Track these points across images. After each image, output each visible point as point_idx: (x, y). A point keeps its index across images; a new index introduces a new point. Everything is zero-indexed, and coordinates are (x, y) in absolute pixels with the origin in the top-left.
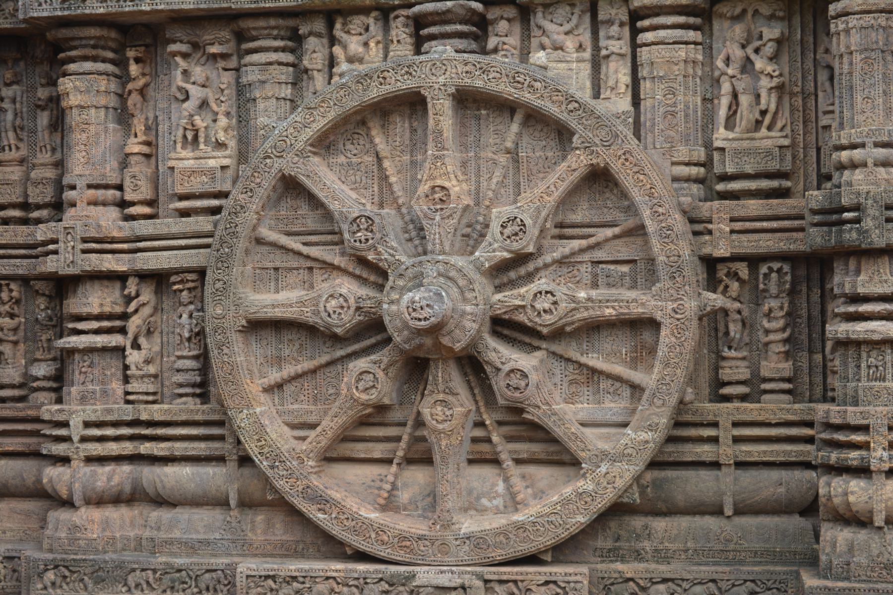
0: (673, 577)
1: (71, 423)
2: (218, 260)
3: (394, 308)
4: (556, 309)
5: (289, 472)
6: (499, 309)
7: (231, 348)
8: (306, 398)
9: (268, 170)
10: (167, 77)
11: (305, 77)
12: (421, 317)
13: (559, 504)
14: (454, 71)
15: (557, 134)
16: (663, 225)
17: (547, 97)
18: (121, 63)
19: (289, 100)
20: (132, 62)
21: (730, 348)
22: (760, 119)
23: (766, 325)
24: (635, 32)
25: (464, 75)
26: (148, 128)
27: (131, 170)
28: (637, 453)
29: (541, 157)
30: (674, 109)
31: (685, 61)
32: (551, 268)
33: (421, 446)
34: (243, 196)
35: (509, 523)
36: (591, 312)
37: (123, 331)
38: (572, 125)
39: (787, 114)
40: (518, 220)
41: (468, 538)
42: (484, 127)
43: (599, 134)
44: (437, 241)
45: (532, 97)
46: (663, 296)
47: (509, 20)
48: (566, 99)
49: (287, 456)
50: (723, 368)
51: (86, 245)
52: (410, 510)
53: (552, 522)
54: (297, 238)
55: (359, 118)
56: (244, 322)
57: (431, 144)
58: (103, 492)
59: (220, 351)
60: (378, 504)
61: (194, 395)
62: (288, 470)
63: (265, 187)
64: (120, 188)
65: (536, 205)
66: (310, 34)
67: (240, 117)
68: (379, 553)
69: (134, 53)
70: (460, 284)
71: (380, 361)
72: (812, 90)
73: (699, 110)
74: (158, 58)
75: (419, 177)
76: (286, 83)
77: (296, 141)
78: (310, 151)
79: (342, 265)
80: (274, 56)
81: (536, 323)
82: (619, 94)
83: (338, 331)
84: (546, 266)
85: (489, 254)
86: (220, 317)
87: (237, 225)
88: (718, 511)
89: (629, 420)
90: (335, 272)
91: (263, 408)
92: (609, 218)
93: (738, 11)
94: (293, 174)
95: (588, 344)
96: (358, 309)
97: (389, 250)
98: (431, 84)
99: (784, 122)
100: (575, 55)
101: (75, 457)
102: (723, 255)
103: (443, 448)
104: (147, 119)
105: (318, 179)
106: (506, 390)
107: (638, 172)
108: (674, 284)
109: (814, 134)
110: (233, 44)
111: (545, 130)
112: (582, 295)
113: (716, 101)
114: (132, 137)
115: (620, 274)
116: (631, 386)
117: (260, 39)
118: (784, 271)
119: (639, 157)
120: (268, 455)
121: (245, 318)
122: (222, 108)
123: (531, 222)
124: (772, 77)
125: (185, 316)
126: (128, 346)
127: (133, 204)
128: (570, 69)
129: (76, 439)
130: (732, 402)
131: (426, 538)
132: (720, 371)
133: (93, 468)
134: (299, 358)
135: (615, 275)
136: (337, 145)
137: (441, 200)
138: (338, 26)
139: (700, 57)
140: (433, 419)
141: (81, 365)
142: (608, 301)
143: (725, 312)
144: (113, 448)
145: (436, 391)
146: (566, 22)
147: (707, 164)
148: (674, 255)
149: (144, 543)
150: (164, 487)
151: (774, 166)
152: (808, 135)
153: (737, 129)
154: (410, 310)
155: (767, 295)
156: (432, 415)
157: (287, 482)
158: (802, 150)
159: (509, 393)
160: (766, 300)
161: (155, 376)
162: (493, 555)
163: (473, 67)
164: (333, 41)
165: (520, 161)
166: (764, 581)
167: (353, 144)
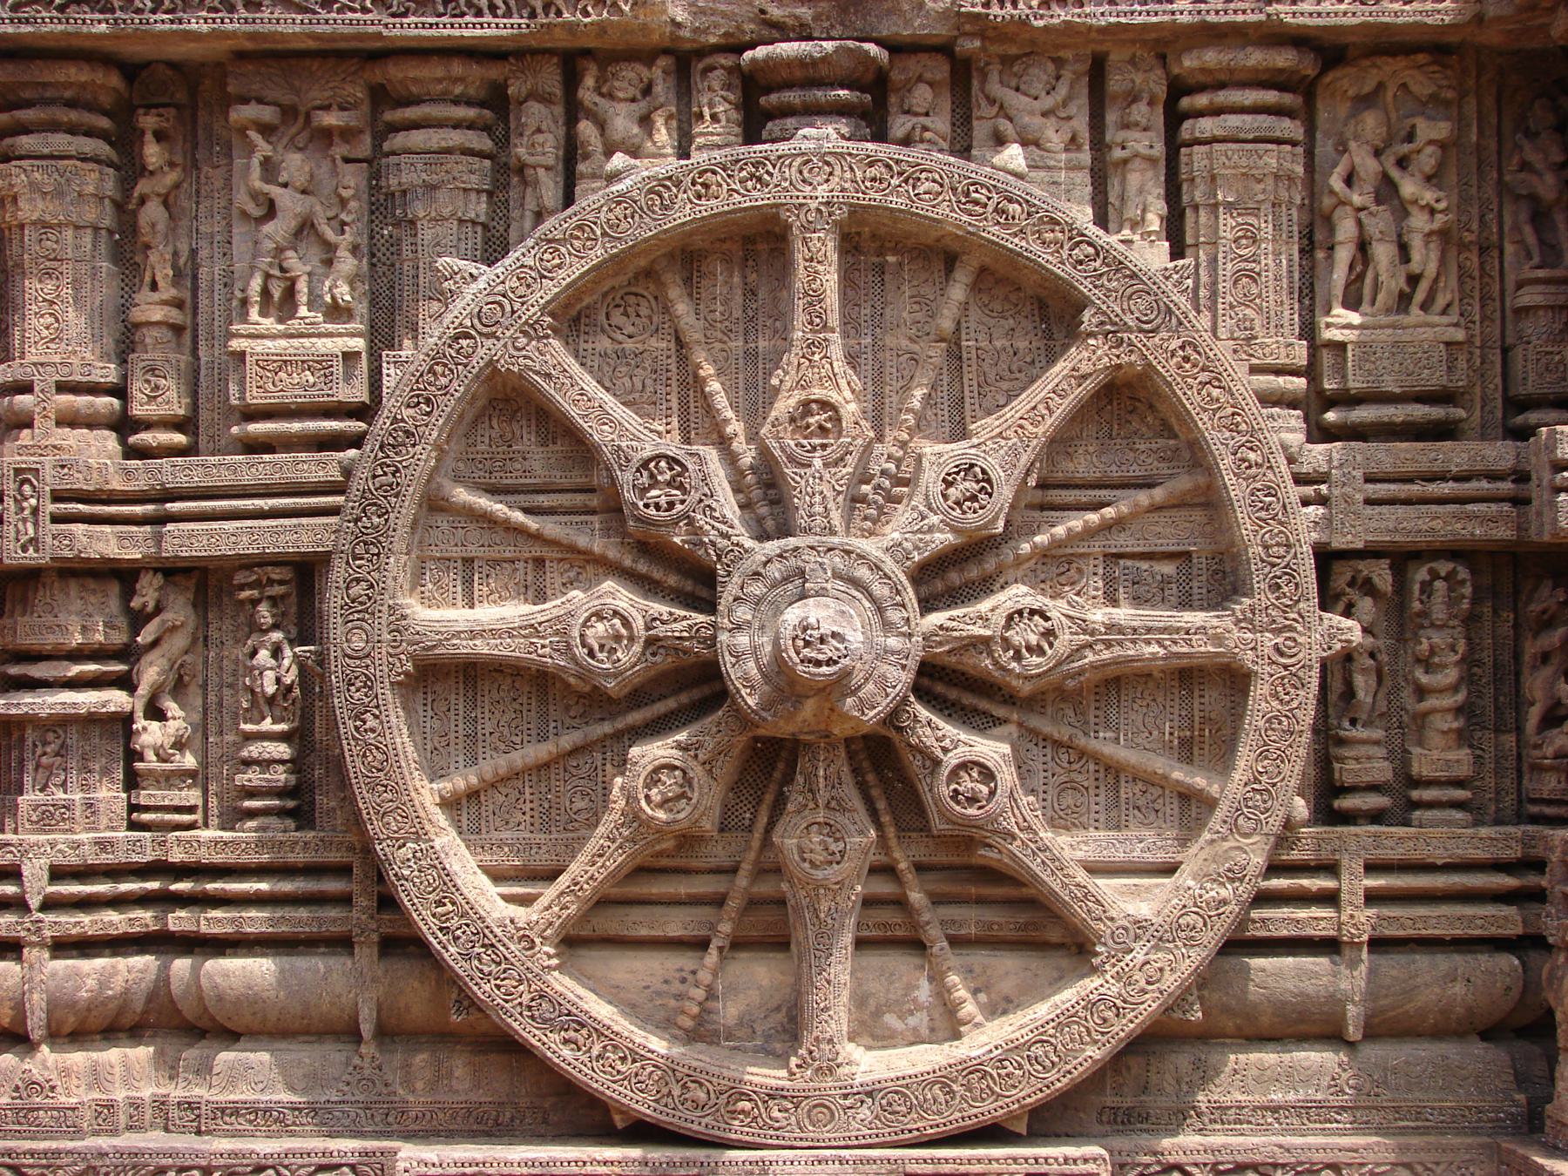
0: (1258, 1158)
1: (26, 871)
2: (358, 538)
3: (743, 640)
4: (1051, 645)
5: (503, 966)
6: (940, 644)
8: (527, 817)
10: (217, 171)
11: (515, 180)
12: (821, 657)
13: (1052, 1024)
14: (848, 175)
15: (1036, 306)
16: (1258, 485)
17: (1033, 234)
18: (125, 142)
19: (482, 224)
20: (149, 137)
21: (1353, 722)
22: (1407, 290)
23: (1424, 679)
24: (1174, 119)
25: (868, 184)
26: (178, 275)
27: (145, 356)
28: (1205, 924)
29: (1004, 349)
31: (1277, 177)
32: (1026, 566)
33: (767, 915)
34: (411, 411)
35: (952, 1061)
37: (126, 683)
38: (1081, 288)
39: (1453, 282)
40: (977, 470)
41: (870, 1094)
42: (894, 288)
43: (1133, 308)
45: (1003, 233)
46: (1257, 623)
47: (931, 84)
48: (1070, 239)
50: (1341, 760)
51: (62, 506)
52: (740, 1039)
53: (1036, 1058)
54: (510, 498)
55: (643, 262)
56: (409, 667)
57: (800, 318)
58: (89, 1010)
59: (358, 723)
60: (680, 1028)
61: (281, 813)
62: (499, 964)
64: (120, 391)
66: (533, 95)
68: (690, 1125)
69: (156, 119)
71: (699, 746)
72: (1495, 238)
73: (1296, 268)
74: (200, 132)
75: (775, 382)
76: (479, 192)
77: (523, 304)
78: (549, 327)
79: (612, 554)
80: (456, 138)
81: (1010, 671)
82: (1150, 233)
83: (611, 684)
84: (1019, 561)
86: (361, 654)
88: (1330, 1034)
89: (1179, 858)
92: (1136, 471)
93: (1368, 88)
95: (1098, 713)
96: (651, 642)
97: (717, 525)
98: (801, 201)
99: (1449, 297)
100: (1064, 156)
101: (34, 938)
102: (1352, 546)
103: (822, 915)
104: (176, 254)
106: (952, 804)
107: (1210, 383)
108: (1278, 598)
109: (1498, 322)
110: (366, 108)
111: (1013, 298)
112: (1099, 615)
113: (1320, 255)
114: (146, 289)
115: (1159, 578)
116: (1180, 795)
117: (424, 101)
118: (1460, 577)
119: (1211, 354)
120: (459, 933)
121: (413, 657)
122: (347, 236)
123: (1002, 474)
124: (1432, 212)
125: (264, 656)
126: (139, 714)
127: (148, 425)
128: (1054, 183)
129: (34, 902)
130: (1355, 824)
131: (785, 1093)
132: (1337, 766)
133: (70, 962)
134: (514, 738)
136: (593, 317)
137: (821, 427)
138: (589, 82)
139: (1300, 170)
140: (804, 860)
141: (39, 751)
143: (1347, 657)
144: (114, 921)
145: (811, 805)
146: (1044, 93)
147: (1310, 371)
148: (1278, 544)
149: (175, 1113)
150: (220, 998)
151: (1434, 379)
152: (1486, 323)
153: (1365, 307)
154: (801, 643)
155: (1426, 623)
156: (801, 851)
157: (498, 987)
158: (1478, 352)
159: (958, 808)
160: (1422, 632)
161: (192, 774)
162: (919, 1124)
163: (883, 170)
164: (573, 112)
165: (965, 356)
166: (1430, 1166)
167: (626, 314)
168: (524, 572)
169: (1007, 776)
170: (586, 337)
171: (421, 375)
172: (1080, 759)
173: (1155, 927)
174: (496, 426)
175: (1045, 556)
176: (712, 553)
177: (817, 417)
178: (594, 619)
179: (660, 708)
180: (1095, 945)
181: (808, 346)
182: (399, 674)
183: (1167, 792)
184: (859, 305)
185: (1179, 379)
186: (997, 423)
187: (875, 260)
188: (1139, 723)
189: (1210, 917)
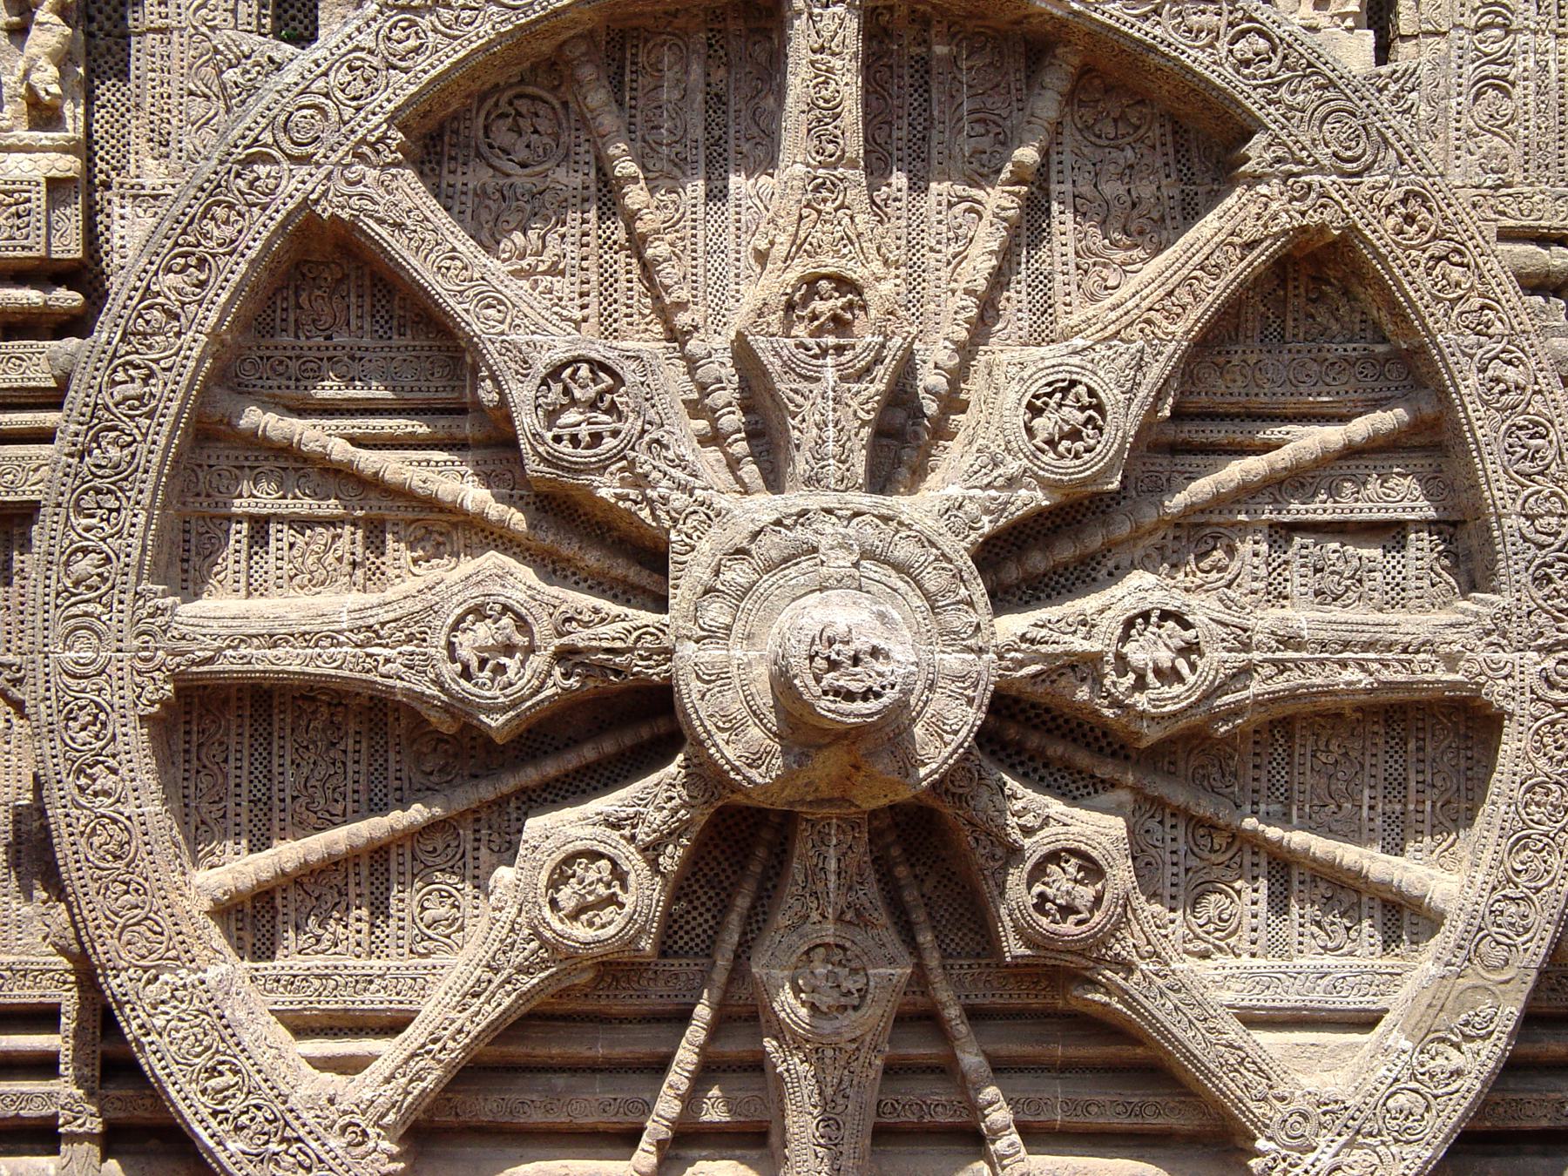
3: (712, 654)
4: (1193, 667)
7: (123, 771)
9: (266, 200)
12: (854, 686)
15: (1168, 127)
16: (1520, 421)
28: (1428, 1109)
30: (1506, 68)
32: (1148, 541)
36: (1295, 678)
38: (1248, 103)
40: (1081, 389)
44: (831, 448)
49: (311, 1121)
55: (546, 47)
59: (83, 781)
63: (251, 254)
65: (1134, 347)
67: (91, 19)
70: (931, 586)
71: (635, 820)
75: (763, 245)
77: (358, 109)
82: (1344, 16)
83: (495, 721)
85: (993, 493)
86: (90, 670)
87: (152, 374)
89: (1381, 1005)
90: (458, 538)
91: (223, 968)
94: (345, 215)
95: (1257, 774)
96: (565, 655)
105: (429, 236)
106: (1036, 916)
107: (1446, 258)
108: (1548, 598)
116: (1385, 904)
119: (1449, 213)
120: (244, 1119)
121: (175, 677)
123: (1121, 397)
135: (1340, 566)
142: (1346, 645)
145: (815, 916)
154: (820, 663)
159: (1044, 921)
168: (350, 541)
169: (1122, 874)
170: (453, 165)
171: (191, 222)
172: (1229, 845)
173: (1350, 1112)
174: (306, 305)
175: (1178, 525)
176: (663, 515)
177: (831, 303)
178: (470, 617)
179: (571, 761)
180: (1255, 1139)
181: (816, 189)
182: (152, 703)
183: (1365, 899)
184: (890, 124)
185: (1399, 251)
186: (1113, 315)
187: (915, 50)
188: (1322, 792)
189: (1436, 1097)
